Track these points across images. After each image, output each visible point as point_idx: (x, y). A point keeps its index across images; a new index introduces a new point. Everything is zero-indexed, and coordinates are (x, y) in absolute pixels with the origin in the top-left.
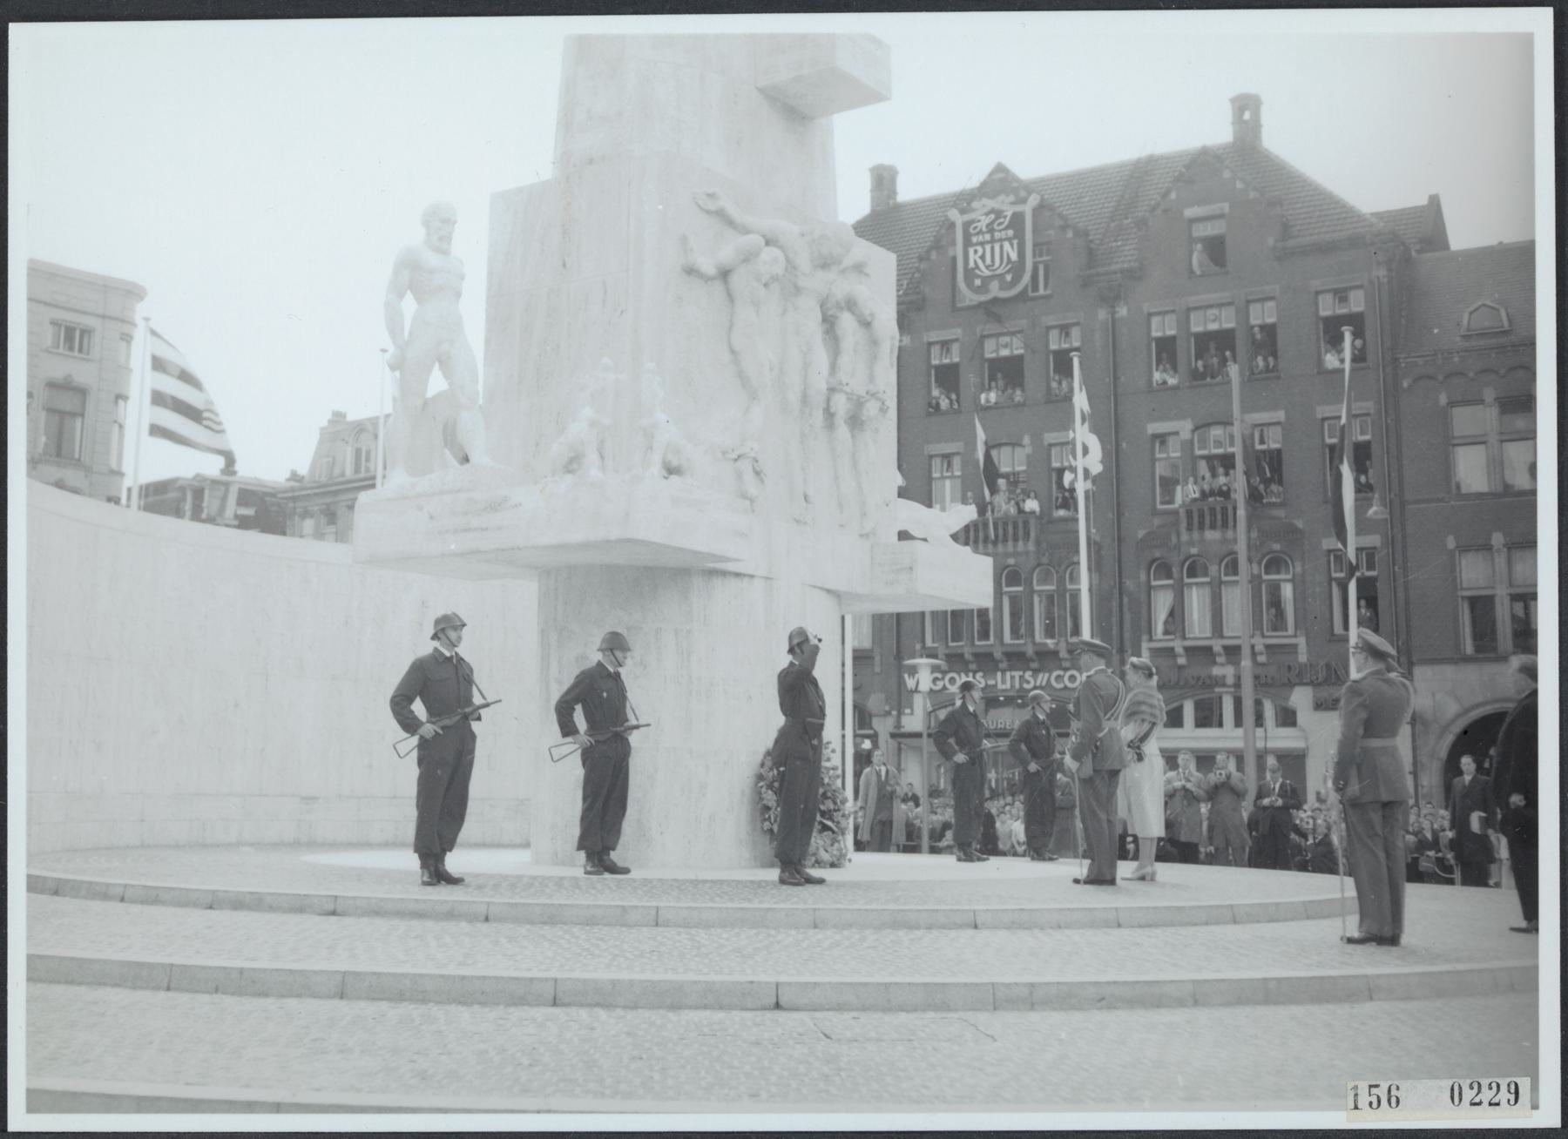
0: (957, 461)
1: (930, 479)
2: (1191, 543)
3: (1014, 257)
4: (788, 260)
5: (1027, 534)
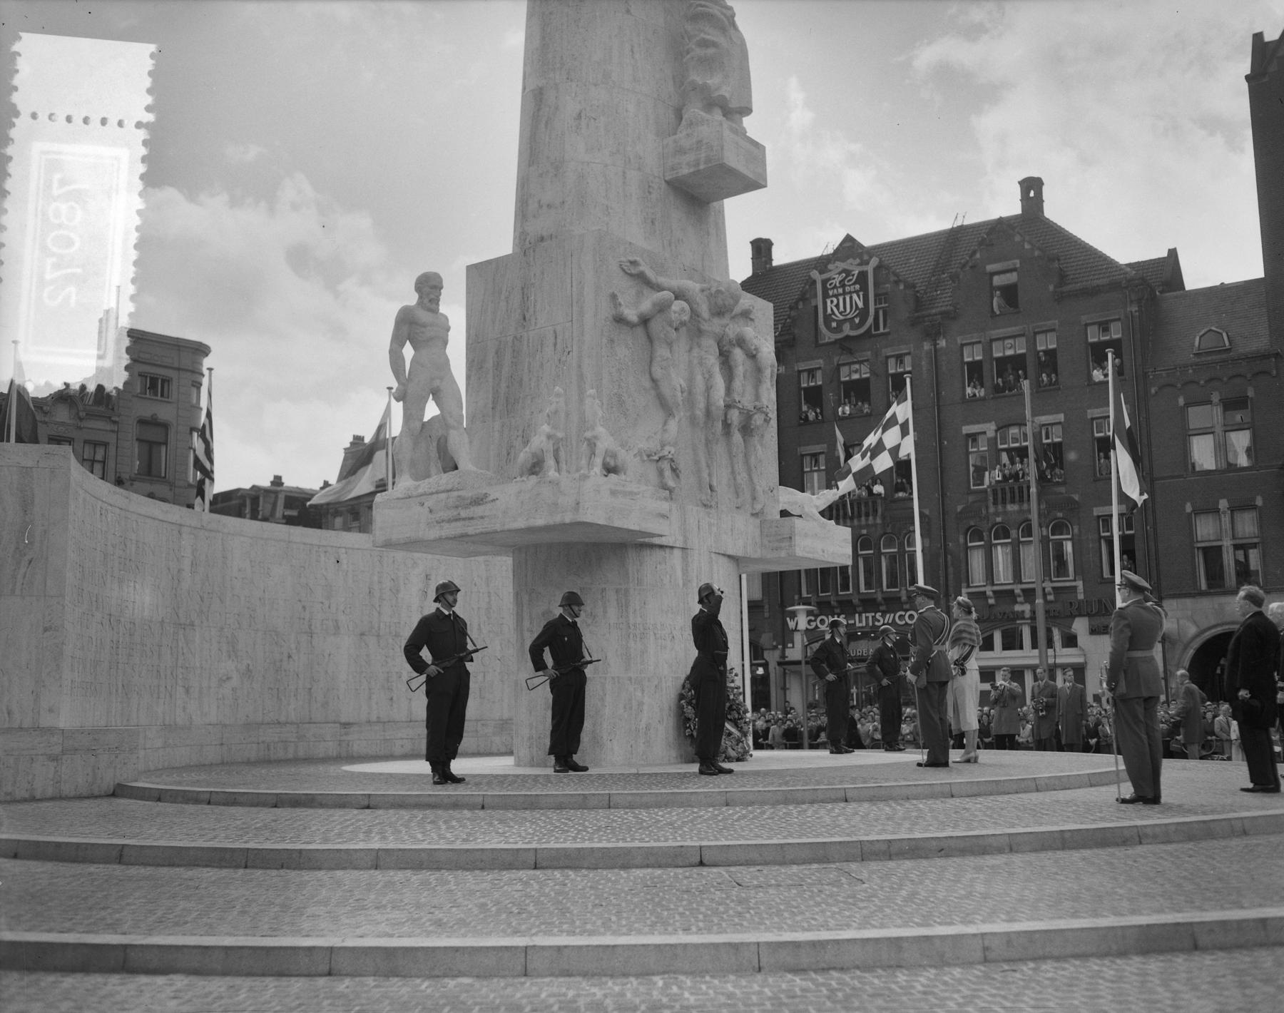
0: (822, 458)
1: (803, 472)
3: (860, 305)
4: (691, 309)
5: (875, 511)
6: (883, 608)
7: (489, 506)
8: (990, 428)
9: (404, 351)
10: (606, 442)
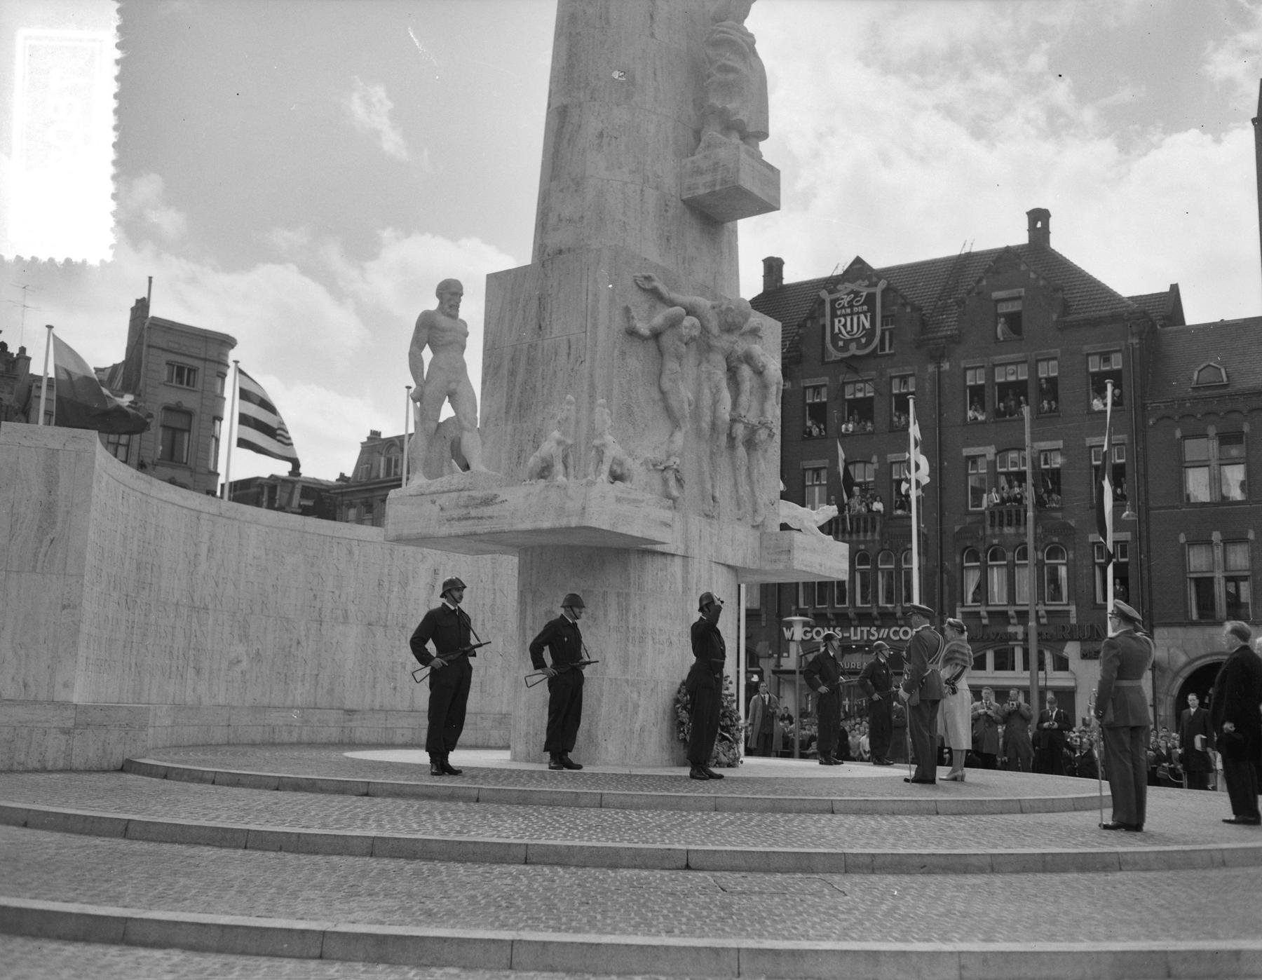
0: (824, 473)
1: (804, 486)
2: (994, 536)
3: (867, 325)
4: (702, 325)
5: (874, 527)
6: (877, 623)
7: (497, 507)
8: (990, 451)
9: (423, 354)
10: (614, 450)
